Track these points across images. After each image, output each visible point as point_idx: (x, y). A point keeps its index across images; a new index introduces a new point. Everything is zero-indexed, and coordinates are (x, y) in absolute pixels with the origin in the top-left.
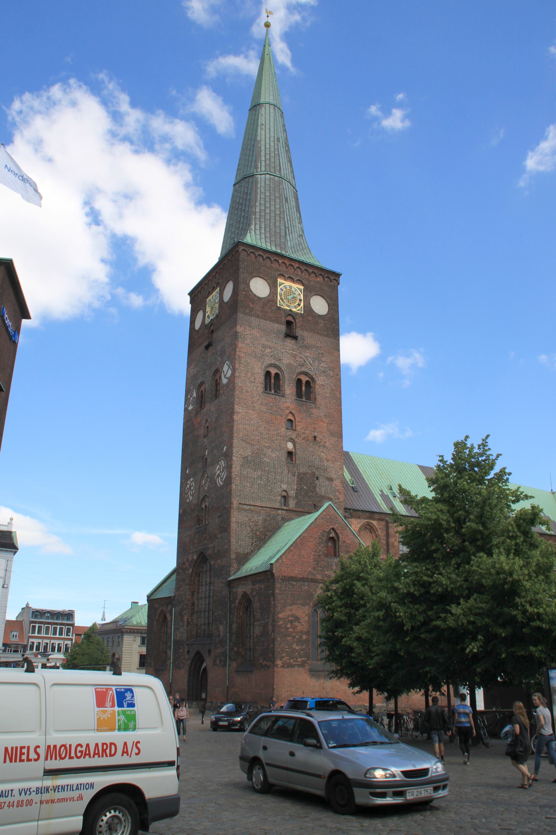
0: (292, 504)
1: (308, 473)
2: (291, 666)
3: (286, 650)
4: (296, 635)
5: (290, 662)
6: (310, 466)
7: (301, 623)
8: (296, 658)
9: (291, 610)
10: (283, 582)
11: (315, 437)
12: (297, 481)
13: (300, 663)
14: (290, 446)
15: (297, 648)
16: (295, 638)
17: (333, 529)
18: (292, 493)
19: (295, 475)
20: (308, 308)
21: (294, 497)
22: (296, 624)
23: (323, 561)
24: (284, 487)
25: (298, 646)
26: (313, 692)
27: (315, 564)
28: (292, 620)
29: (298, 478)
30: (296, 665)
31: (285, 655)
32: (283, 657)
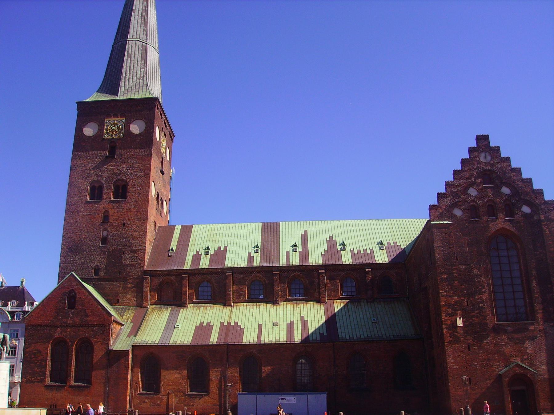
0: (102, 274)
1: (116, 250)
2: (34, 382)
3: (30, 372)
4: (37, 362)
5: (32, 380)
6: (118, 245)
7: (42, 354)
8: (36, 377)
9: (35, 346)
10: (31, 329)
11: (124, 224)
12: (107, 257)
13: (39, 380)
14: (105, 233)
15: (38, 370)
16: (37, 364)
17: (72, 290)
18: (103, 266)
19: (105, 254)
20: (128, 132)
21: (104, 269)
22: (39, 355)
23: (62, 312)
24: (97, 263)
25: (39, 369)
26: (47, 399)
27: (55, 315)
28: (35, 353)
29: (108, 255)
30: (36, 381)
31: (28, 375)
32: (27, 377)
